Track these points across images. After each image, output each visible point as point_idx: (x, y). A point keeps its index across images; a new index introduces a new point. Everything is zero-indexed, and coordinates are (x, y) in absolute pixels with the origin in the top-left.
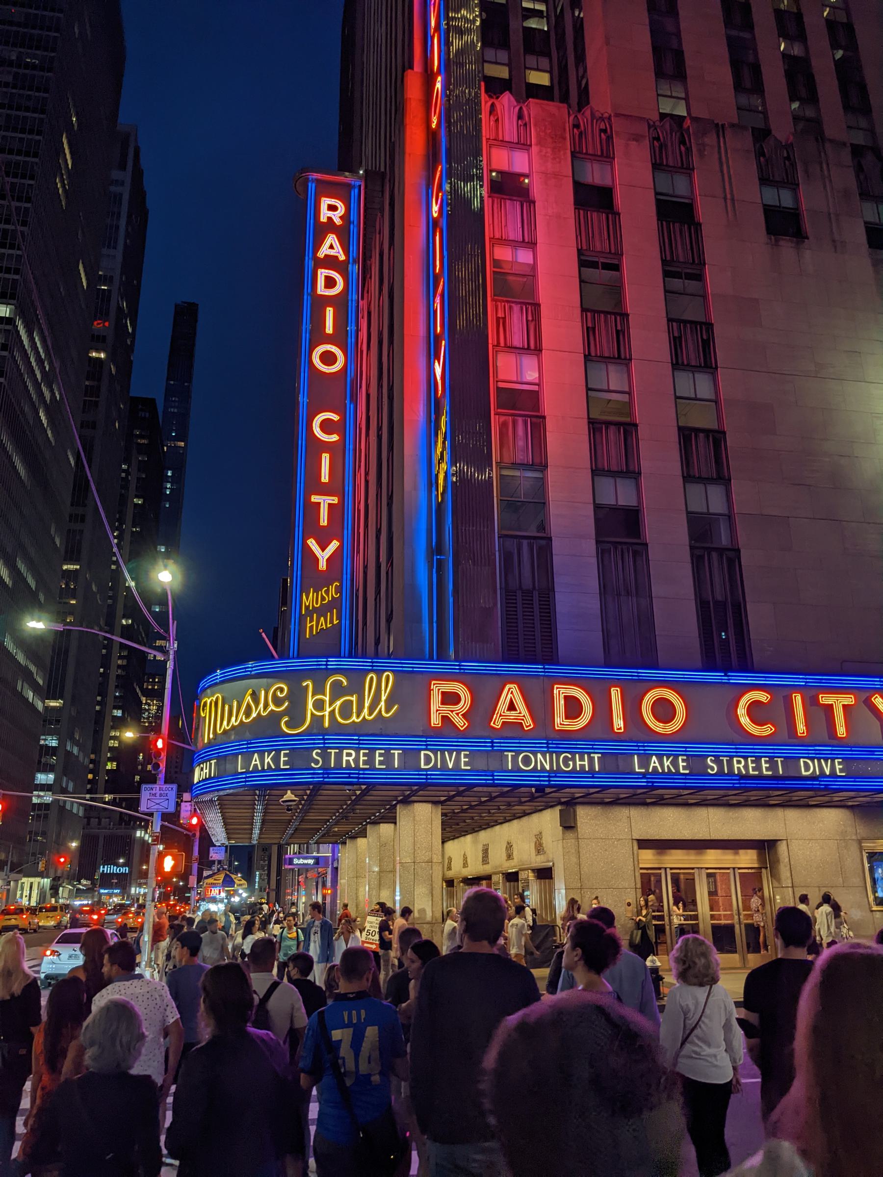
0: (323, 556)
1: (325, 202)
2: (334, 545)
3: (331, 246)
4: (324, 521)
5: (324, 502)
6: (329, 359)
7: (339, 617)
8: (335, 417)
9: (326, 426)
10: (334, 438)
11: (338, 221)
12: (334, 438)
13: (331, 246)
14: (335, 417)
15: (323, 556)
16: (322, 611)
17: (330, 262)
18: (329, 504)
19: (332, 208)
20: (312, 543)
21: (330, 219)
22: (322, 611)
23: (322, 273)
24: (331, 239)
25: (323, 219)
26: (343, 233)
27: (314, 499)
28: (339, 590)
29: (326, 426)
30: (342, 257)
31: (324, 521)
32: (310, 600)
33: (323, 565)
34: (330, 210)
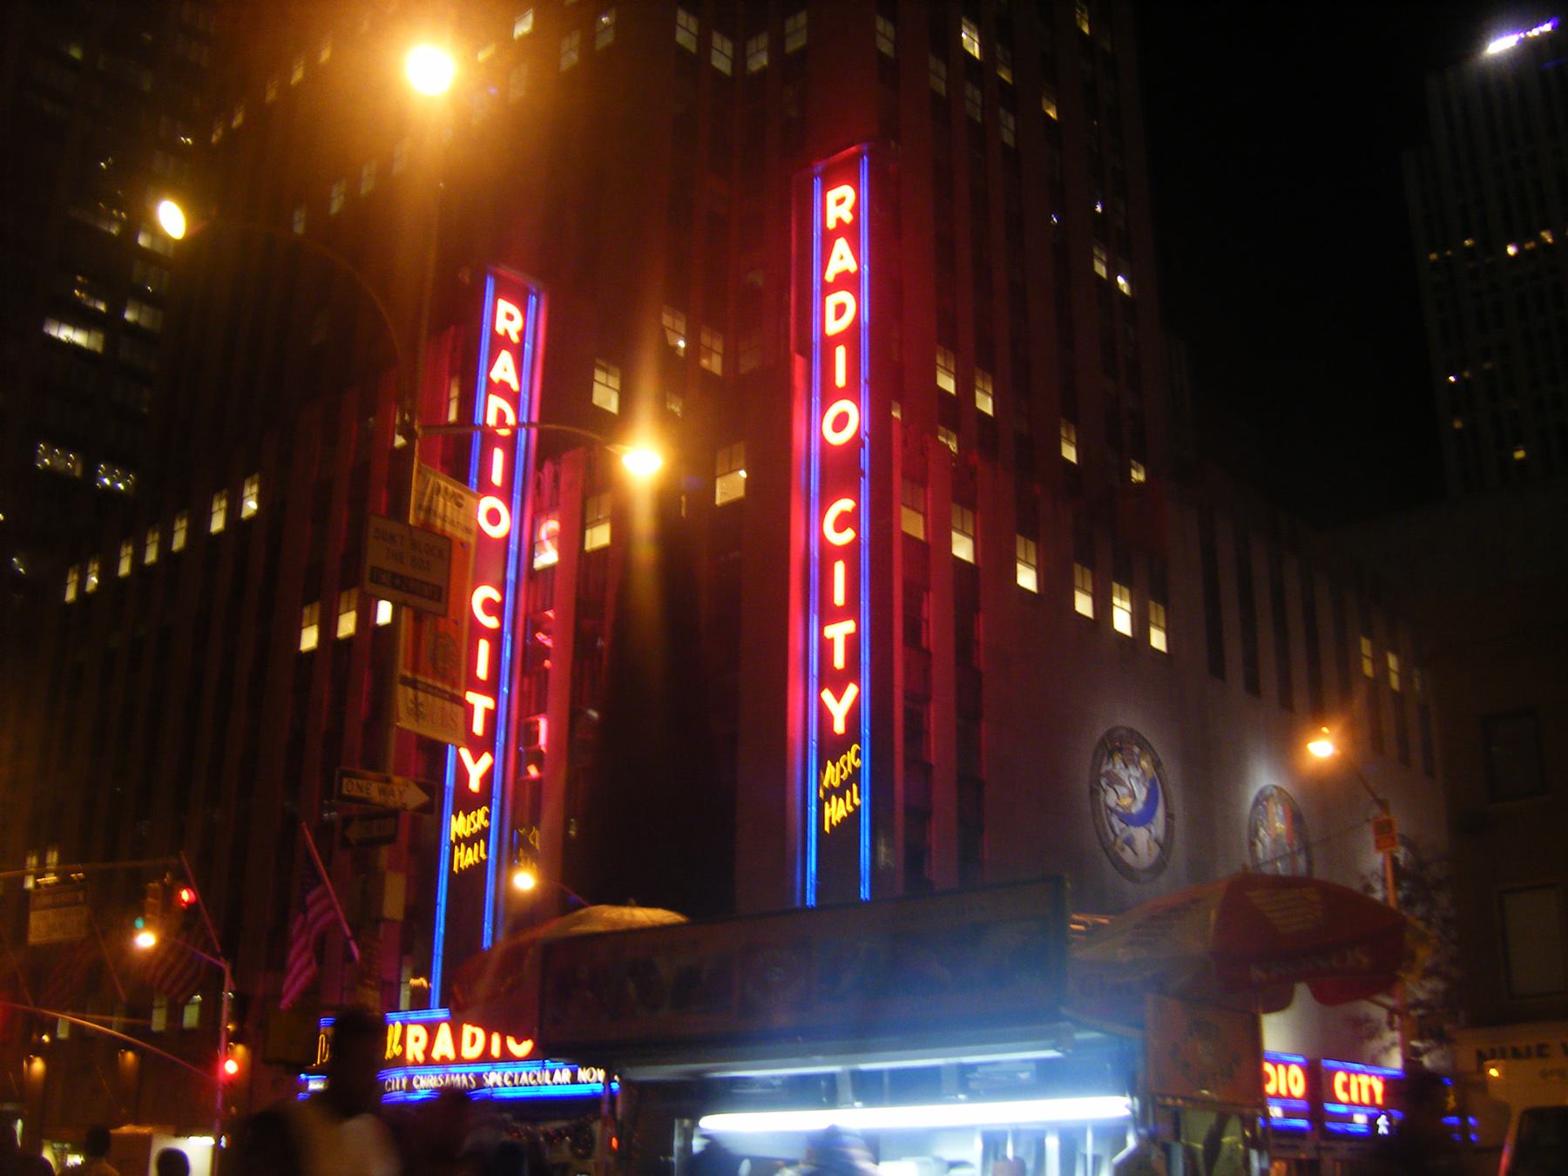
0: (477, 769)
1: (504, 306)
2: (486, 760)
3: (504, 369)
4: (478, 728)
5: (481, 703)
6: (494, 517)
7: (487, 852)
8: (497, 597)
9: (489, 607)
10: (491, 622)
11: (515, 339)
12: (491, 622)
13: (504, 369)
14: (497, 597)
15: (477, 769)
16: (469, 841)
17: (502, 389)
18: (488, 711)
19: (510, 317)
20: (465, 754)
21: (506, 332)
22: (469, 841)
23: (496, 403)
24: (505, 360)
25: (500, 330)
26: (518, 353)
27: (471, 697)
28: (488, 816)
29: (489, 607)
30: (515, 387)
31: (478, 728)
32: (459, 826)
33: (474, 785)
34: (507, 318)
